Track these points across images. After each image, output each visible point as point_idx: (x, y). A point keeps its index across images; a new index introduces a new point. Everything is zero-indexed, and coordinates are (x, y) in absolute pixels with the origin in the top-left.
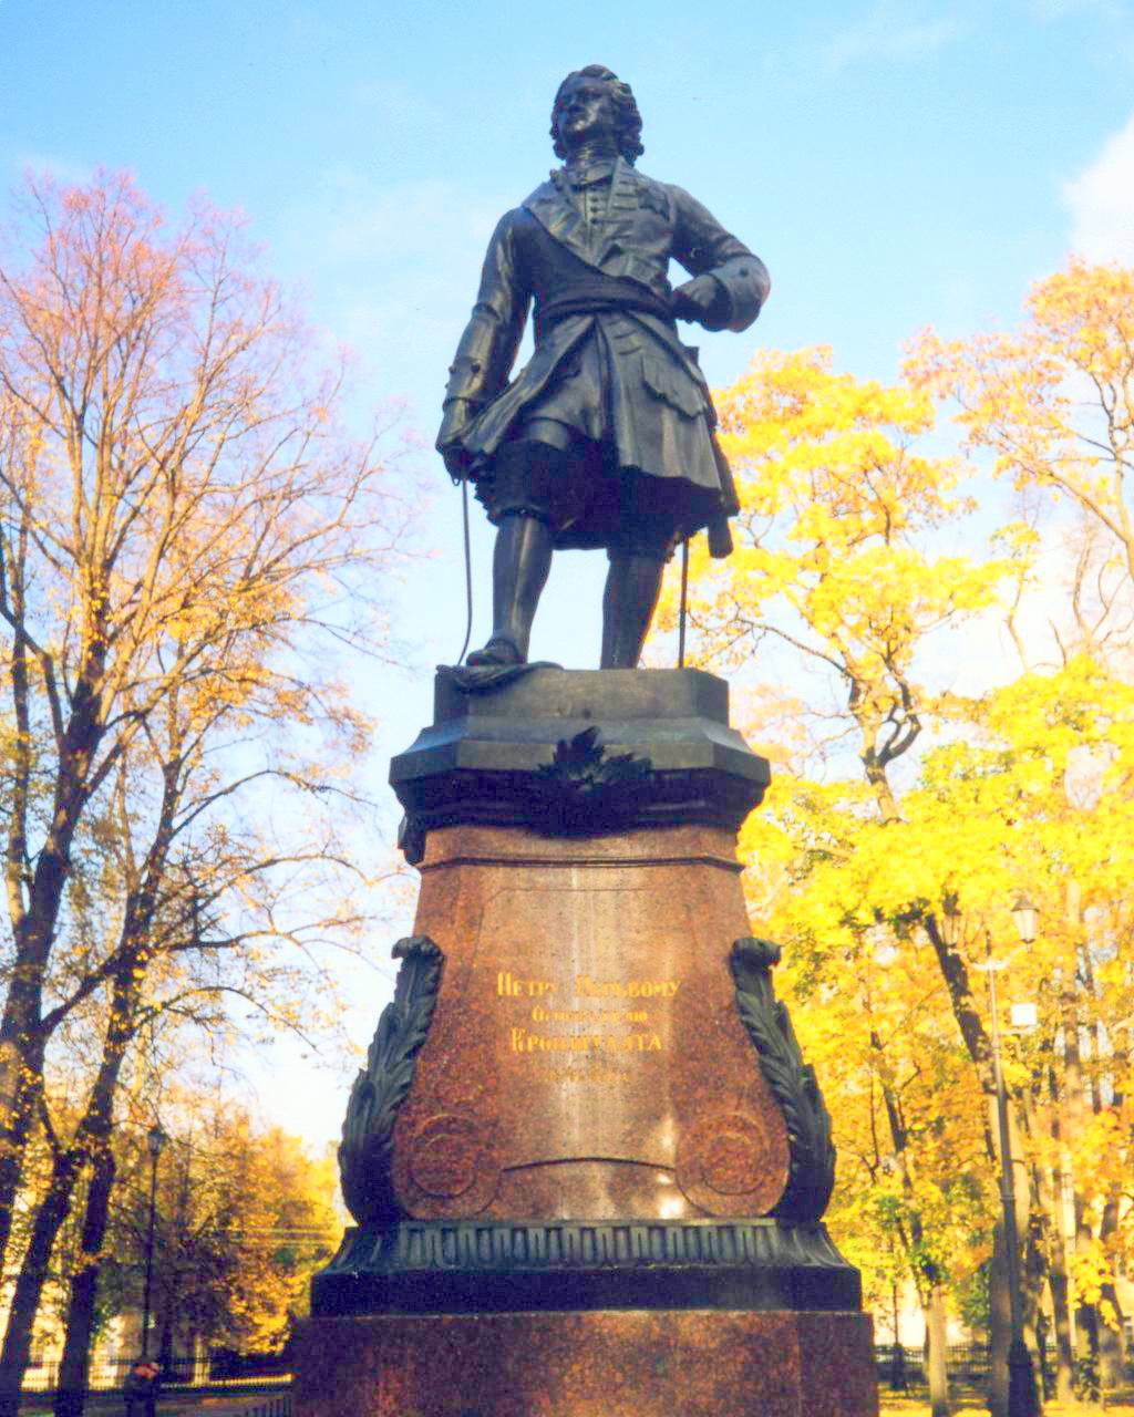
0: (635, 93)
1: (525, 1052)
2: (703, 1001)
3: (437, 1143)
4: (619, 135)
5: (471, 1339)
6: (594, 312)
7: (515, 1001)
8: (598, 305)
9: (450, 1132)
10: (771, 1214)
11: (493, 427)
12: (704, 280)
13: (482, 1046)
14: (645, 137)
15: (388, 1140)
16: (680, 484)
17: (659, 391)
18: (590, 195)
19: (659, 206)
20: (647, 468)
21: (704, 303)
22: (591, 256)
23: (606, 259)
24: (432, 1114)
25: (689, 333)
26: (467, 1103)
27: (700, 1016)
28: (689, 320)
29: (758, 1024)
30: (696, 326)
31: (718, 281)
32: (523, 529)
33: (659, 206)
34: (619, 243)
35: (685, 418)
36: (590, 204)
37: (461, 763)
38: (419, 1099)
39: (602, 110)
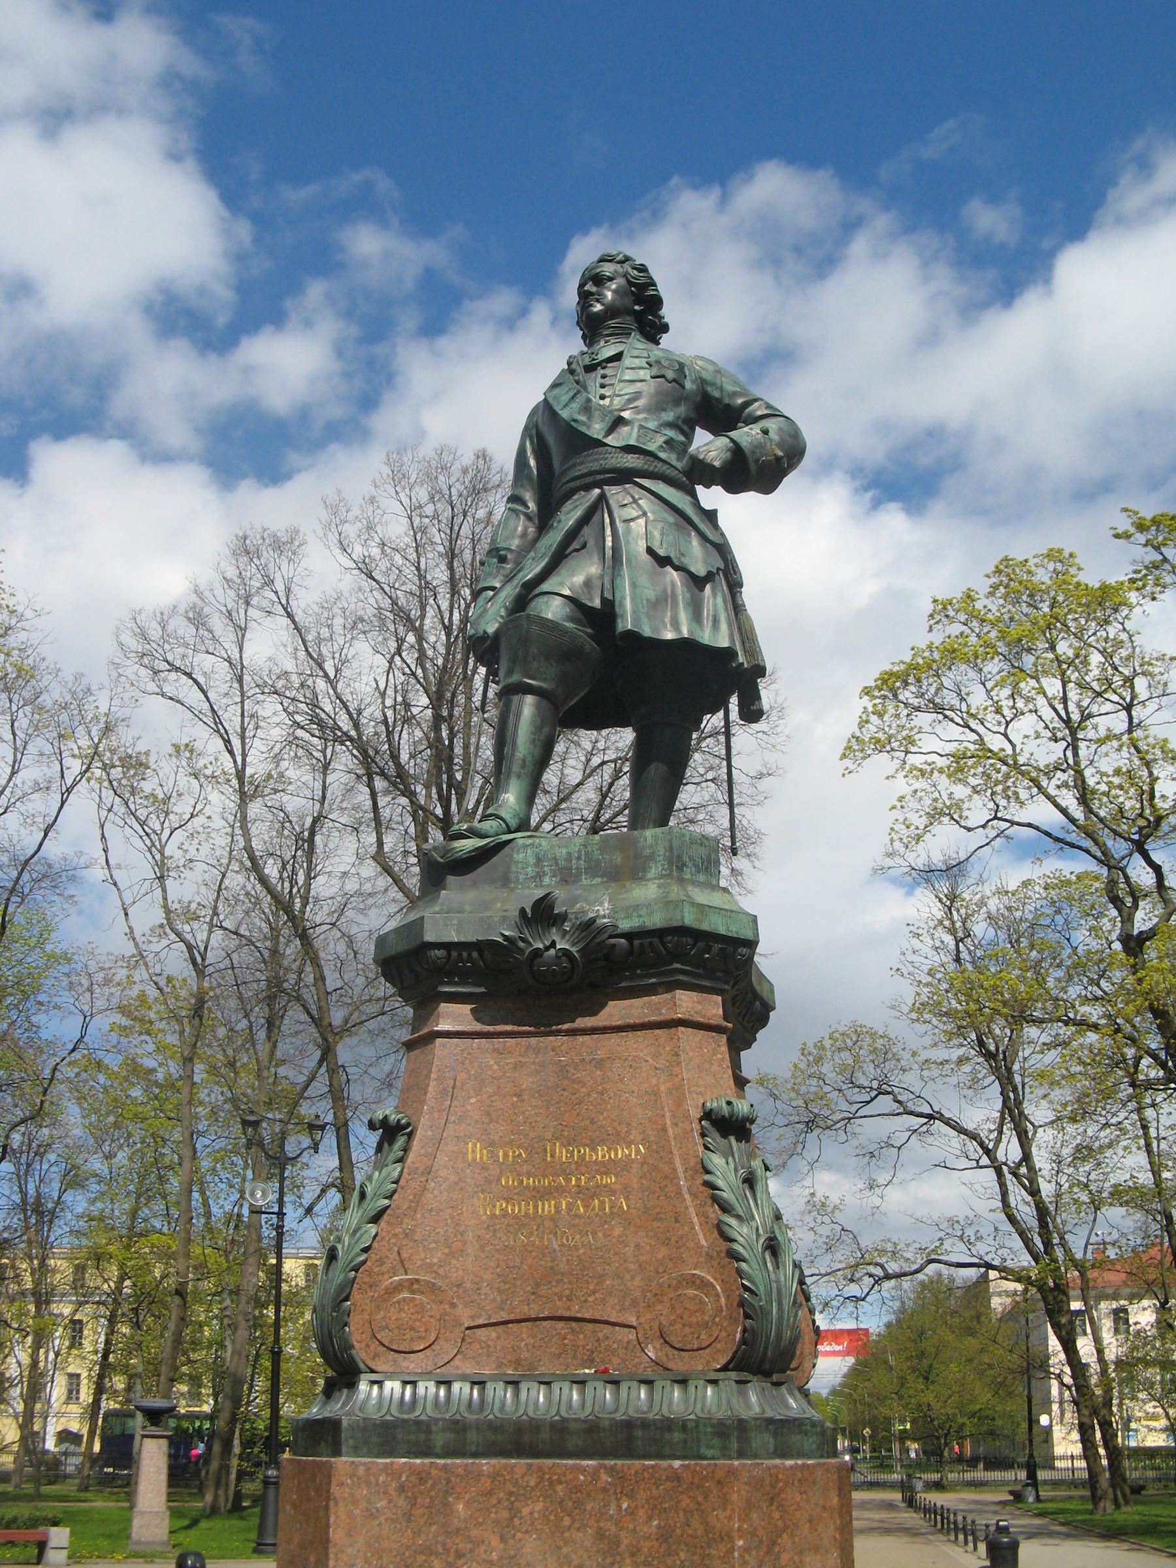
0: (654, 273)
1: (493, 1216)
2: (671, 1162)
3: (398, 1302)
4: (639, 318)
5: (422, 1481)
6: (598, 484)
7: (484, 1167)
8: (602, 477)
9: (413, 1292)
10: (725, 1368)
12: (722, 441)
13: (449, 1211)
14: (668, 312)
15: (346, 1299)
16: (687, 646)
17: (661, 552)
18: (600, 372)
19: (670, 375)
20: (647, 631)
21: (717, 464)
22: (596, 430)
23: (611, 430)
24: (395, 1275)
25: (711, 497)
26: (431, 1265)
27: (666, 1177)
28: (708, 486)
29: (720, 1183)
30: (717, 490)
31: (732, 440)
32: (521, 702)
33: (670, 375)
34: (626, 415)
36: (599, 381)
37: (429, 937)
38: (381, 1262)
39: (615, 292)
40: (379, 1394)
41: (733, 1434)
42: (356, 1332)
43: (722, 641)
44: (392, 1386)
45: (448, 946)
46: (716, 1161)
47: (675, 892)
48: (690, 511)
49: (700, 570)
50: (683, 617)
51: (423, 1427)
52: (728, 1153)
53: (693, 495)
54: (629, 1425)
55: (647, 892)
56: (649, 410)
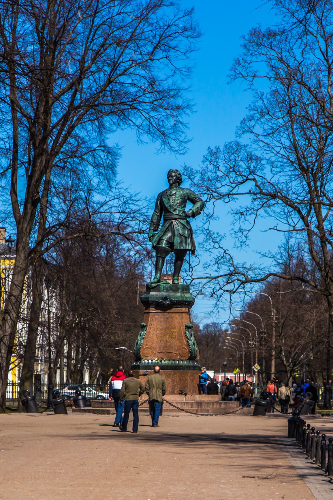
11: (155, 241)
20: (179, 248)
22: (172, 210)
35: (186, 238)
40: (145, 361)
41: (189, 368)
42: (141, 354)
43: (190, 248)
44: (146, 361)
45: (152, 301)
46: (187, 332)
47: (183, 295)
48: (186, 225)
49: (186, 236)
50: (184, 245)
51: (150, 366)
52: (188, 331)
53: (186, 219)
54: (176, 366)
55: (179, 294)
56: (179, 205)
